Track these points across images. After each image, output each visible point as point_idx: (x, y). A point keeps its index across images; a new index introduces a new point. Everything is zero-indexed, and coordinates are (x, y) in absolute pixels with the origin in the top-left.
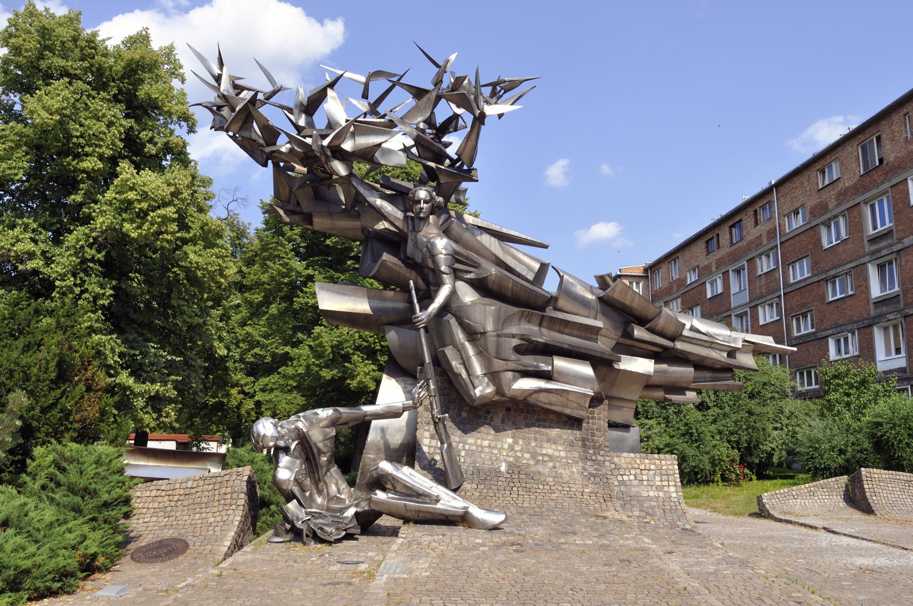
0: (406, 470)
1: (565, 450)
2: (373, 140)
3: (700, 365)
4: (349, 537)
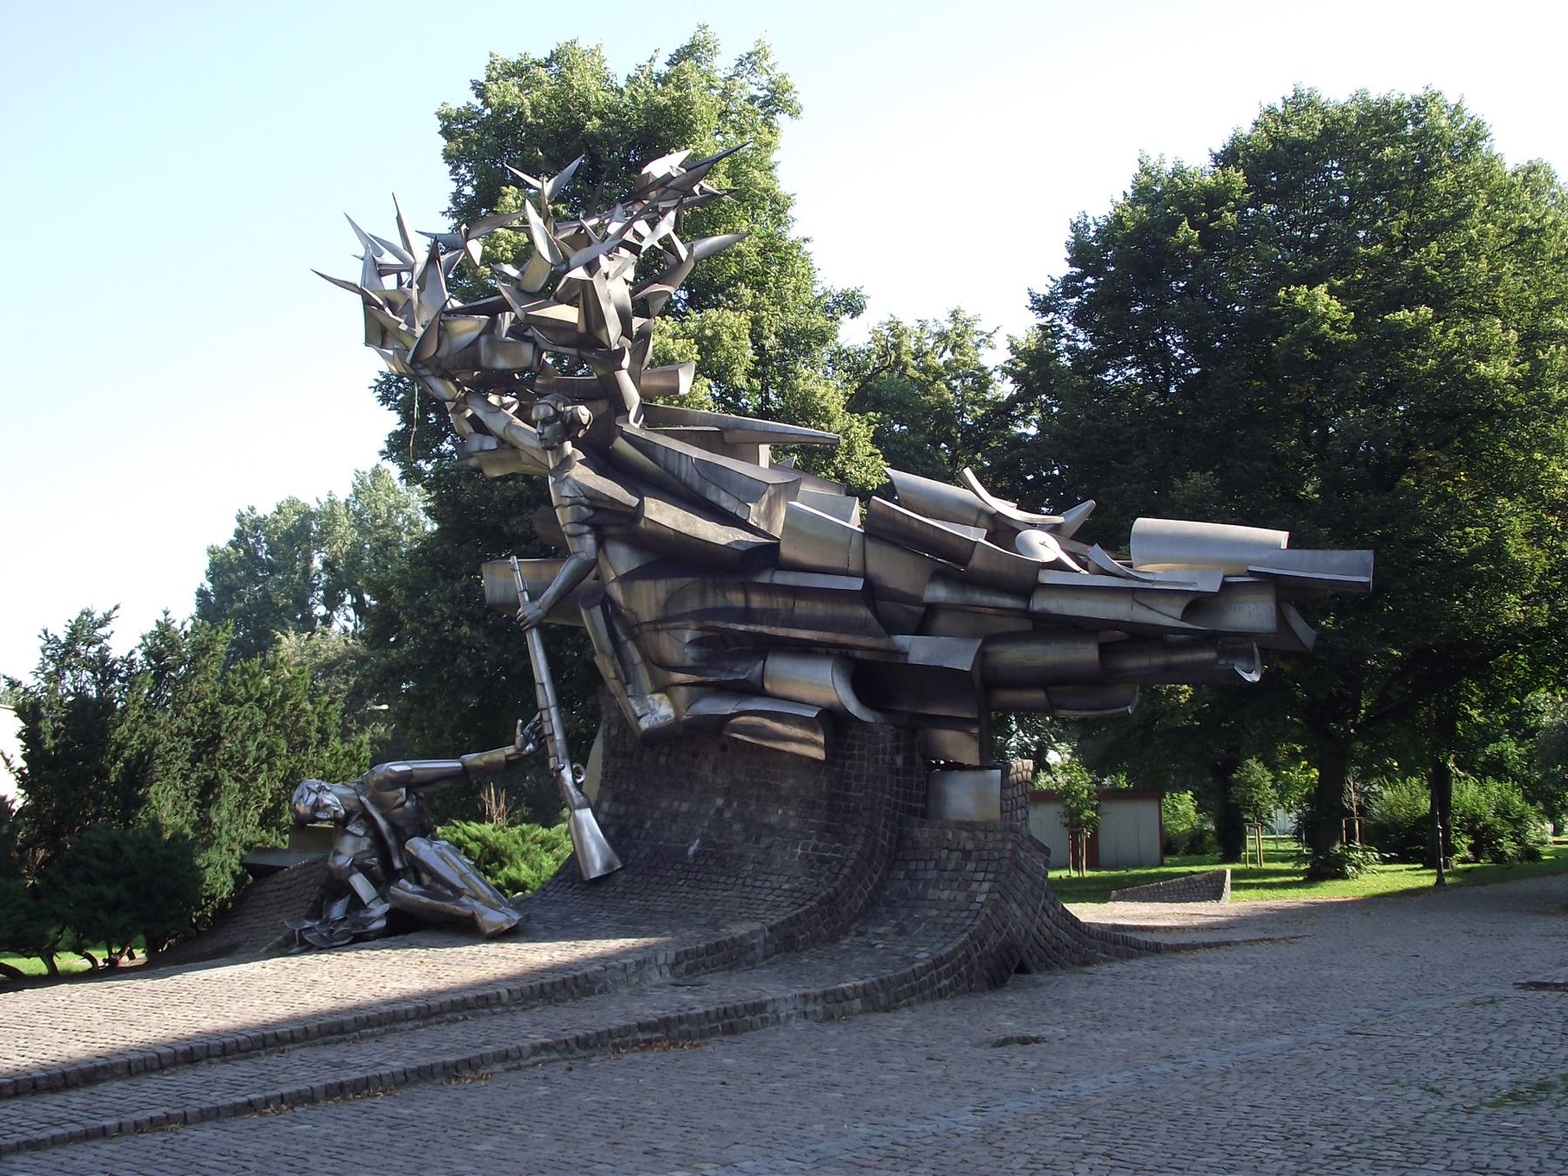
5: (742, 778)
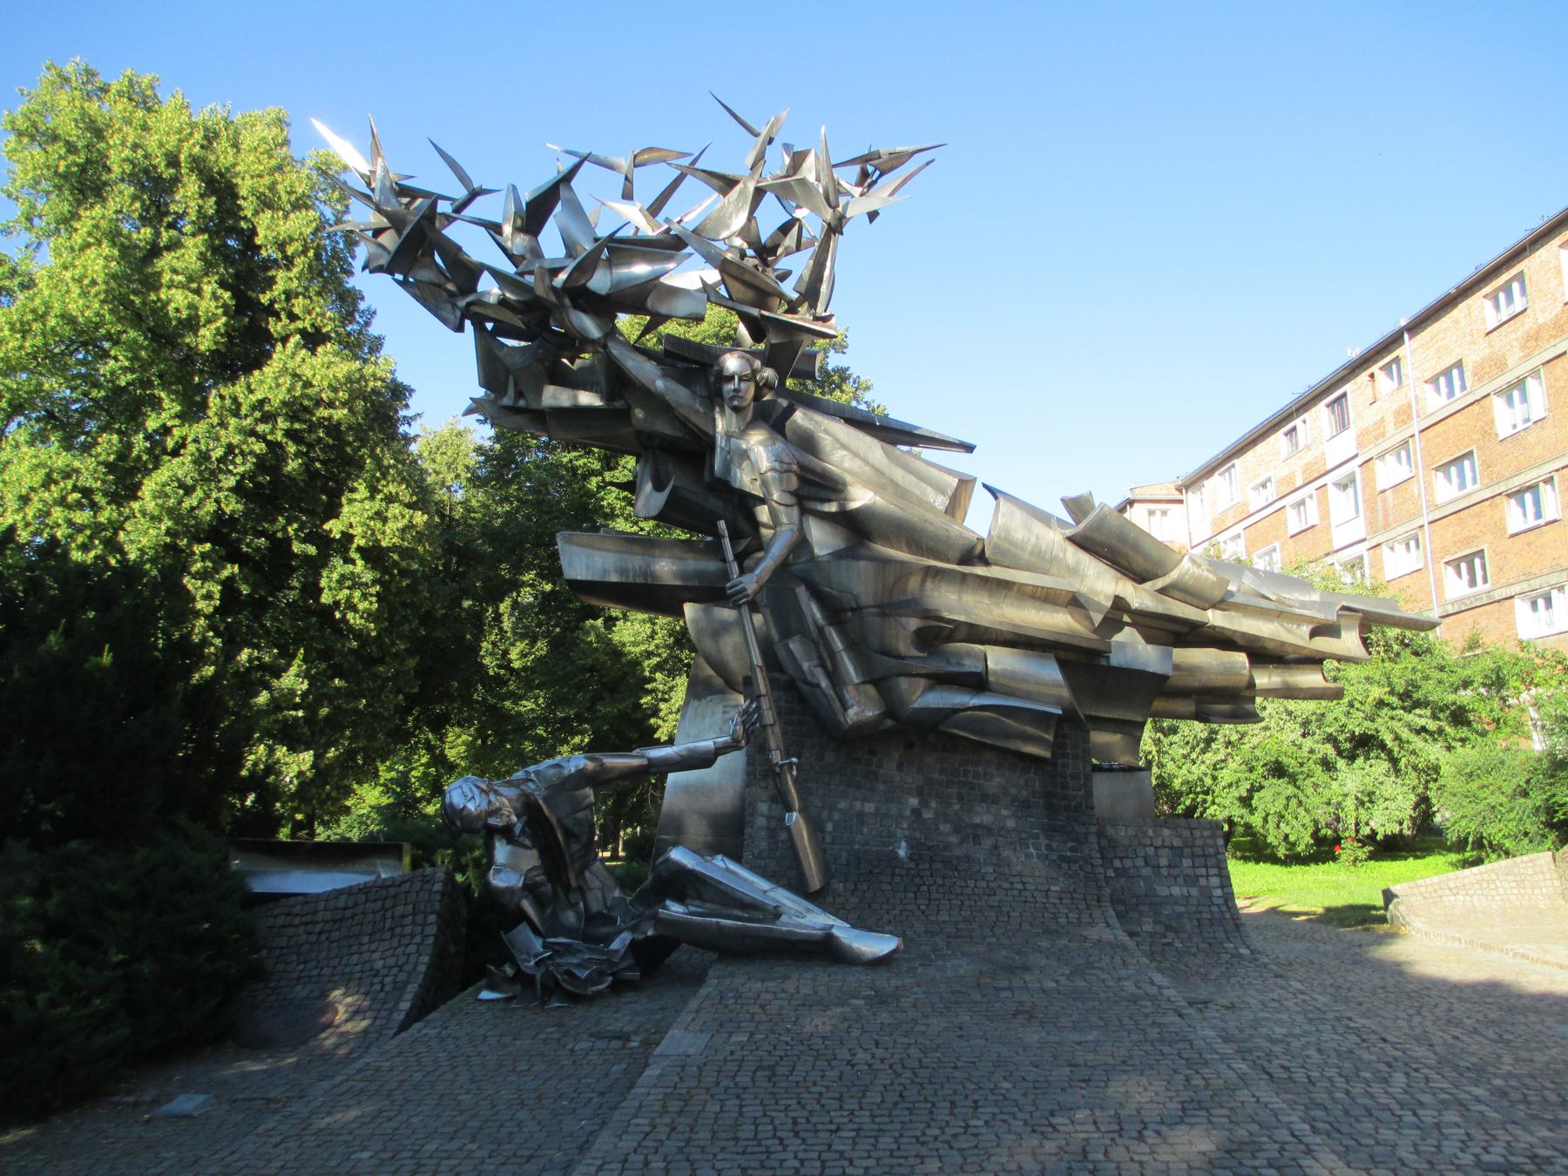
0: (720, 861)
1: (1015, 815)
2: (641, 269)
3: (1262, 654)
4: (620, 986)
5: (936, 776)
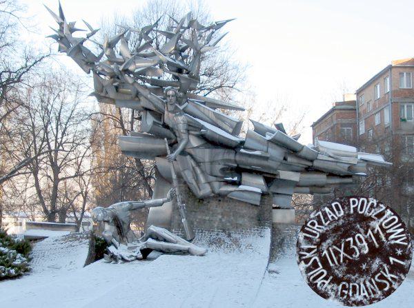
3: (331, 174)
